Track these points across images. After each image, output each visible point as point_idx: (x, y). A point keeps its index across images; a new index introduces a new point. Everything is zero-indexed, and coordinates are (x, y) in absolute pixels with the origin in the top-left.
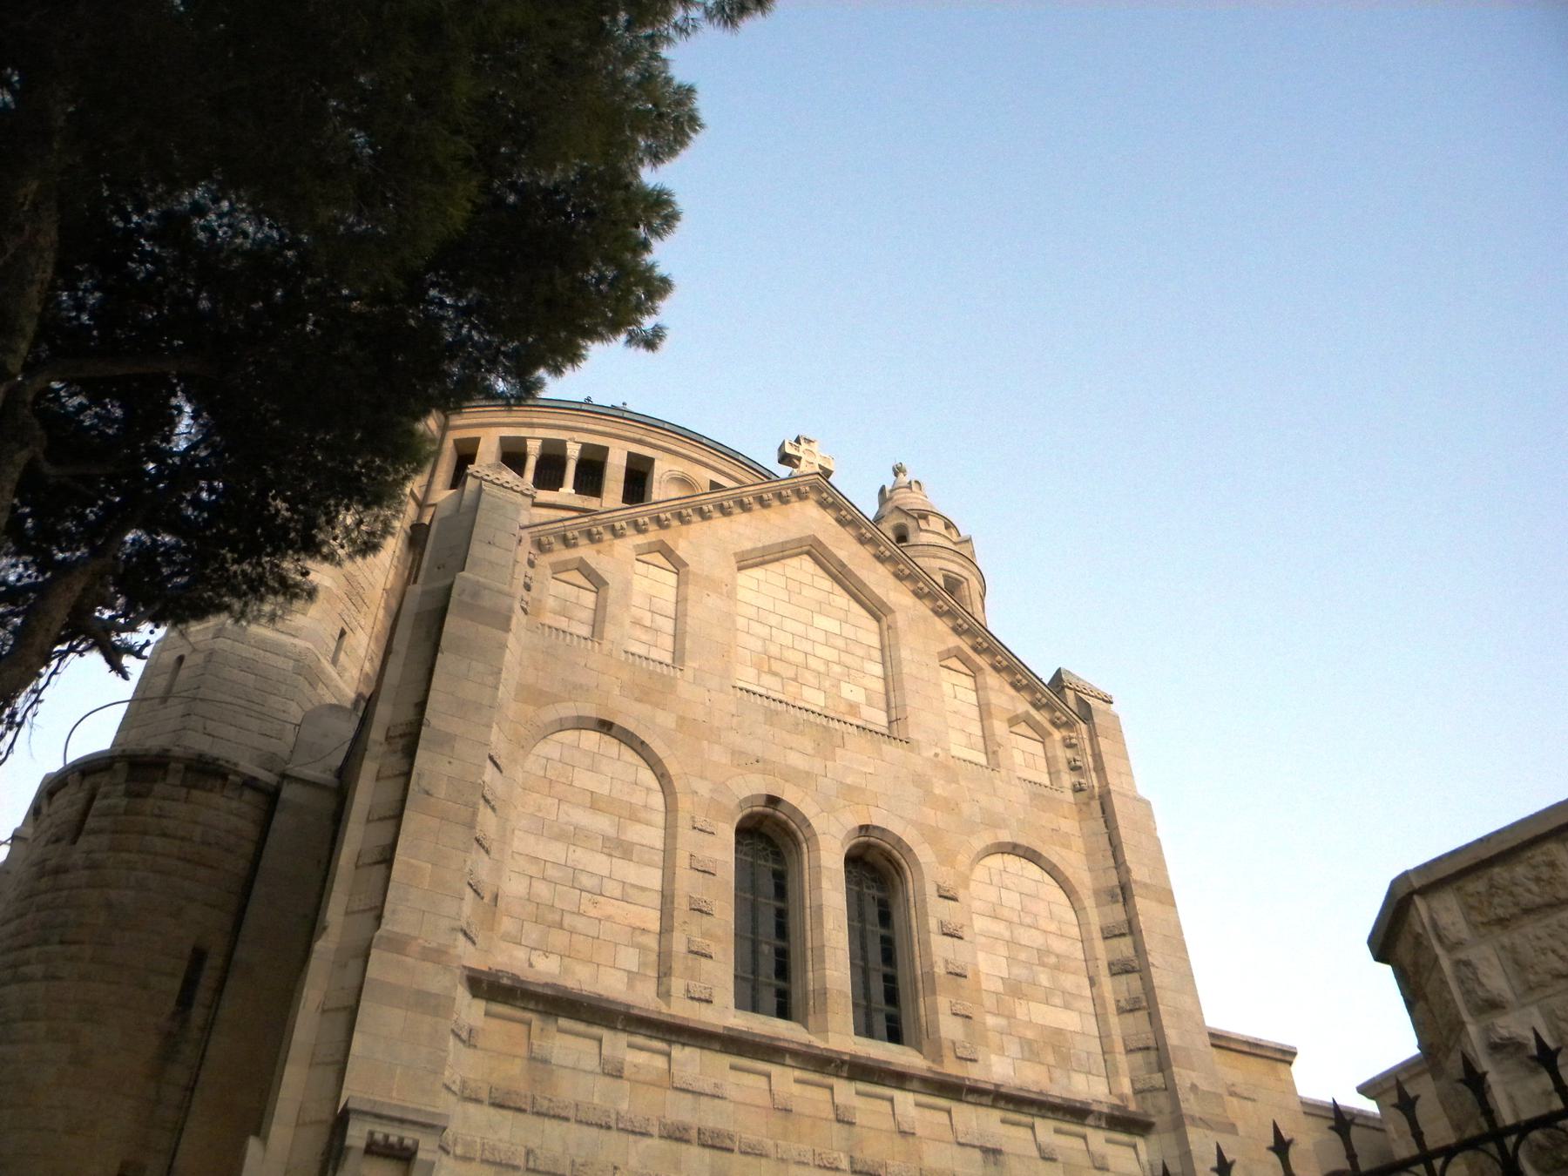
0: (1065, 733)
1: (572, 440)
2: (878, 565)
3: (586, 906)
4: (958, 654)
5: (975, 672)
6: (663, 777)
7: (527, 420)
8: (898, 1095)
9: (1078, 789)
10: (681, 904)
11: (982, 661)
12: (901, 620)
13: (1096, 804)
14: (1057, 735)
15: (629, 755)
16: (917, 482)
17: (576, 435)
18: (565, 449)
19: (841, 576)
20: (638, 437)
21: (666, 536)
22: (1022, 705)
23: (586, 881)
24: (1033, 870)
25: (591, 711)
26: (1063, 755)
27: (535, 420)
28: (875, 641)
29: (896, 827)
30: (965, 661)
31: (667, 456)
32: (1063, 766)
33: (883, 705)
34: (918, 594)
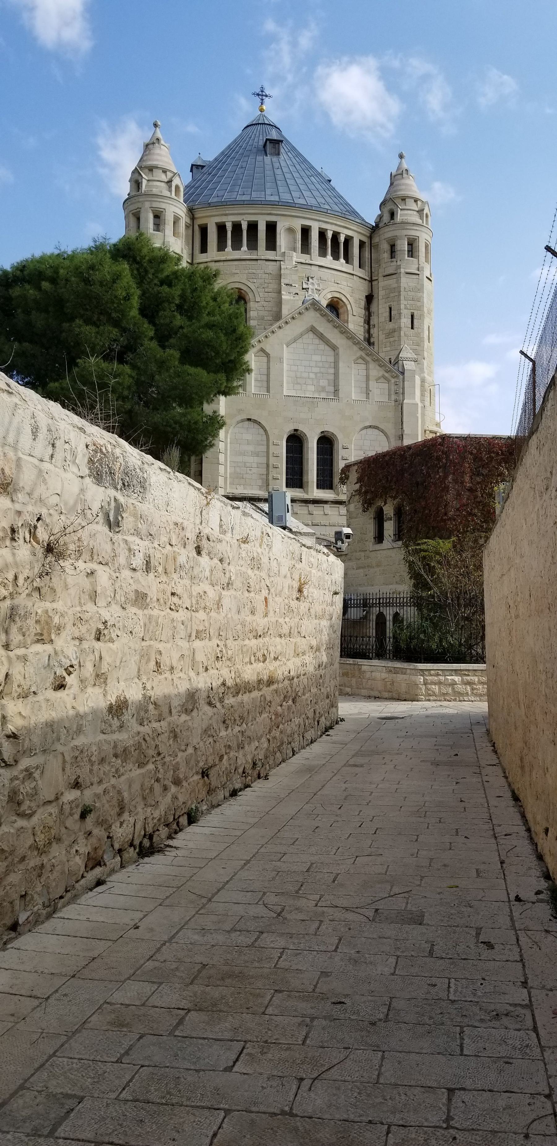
0: (396, 380)
1: (243, 220)
2: (335, 329)
3: (248, 471)
4: (361, 358)
5: (367, 363)
6: (265, 431)
7: (224, 212)
8: (325, 505)
9: (396, 401)
10: (271, 466)
11: (368, 358)
12: (341, 351)
13: (400, 406)
14: (393, 380)
15: (256, 426)
16: (406, 170)
17: (244, 217)
18: (241, 225)
19: (321, 337)
20: (269, 212)
21: (261, 345)
22: (382, 372)
23: (248, 465)
24: (376, 432)
25: (246, 417)
26: (393, 388)
27: (227, 212)
28: (331, 359)
29: (331, 430)
30: (363, 359)
31: (283, 218)
32: (393, 392)
33: (333, 384)
34: (348, 338)
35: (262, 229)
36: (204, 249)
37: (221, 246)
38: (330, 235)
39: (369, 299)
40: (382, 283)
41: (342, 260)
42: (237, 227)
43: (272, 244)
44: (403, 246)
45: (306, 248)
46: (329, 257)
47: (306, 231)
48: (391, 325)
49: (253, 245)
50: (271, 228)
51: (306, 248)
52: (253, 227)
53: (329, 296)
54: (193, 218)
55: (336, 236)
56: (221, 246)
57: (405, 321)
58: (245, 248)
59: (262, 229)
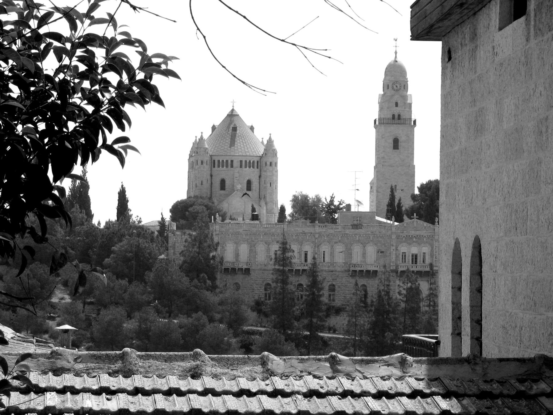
35: (229, 162)
36: (214, 167)
37: (219, 166)
38: (248, 161)
39: (260, 177)
40: (263, 173)
41: (252, 168)
42: (223, 161)
43: (232, 166)
44: (268, 163)
45: (241, 167)
46: (248, 168)
47: (241, 161)
48: (265, 185)
49: (227, 167)
50: (232, 161)
51: (241, 167)
52: (227, 161)
53: (248, 179)
54: (211, 158)
55: (250, 161)
56: (219, 166)
57: (269, 185)
58: (225, 167)
59: (229, 162)
